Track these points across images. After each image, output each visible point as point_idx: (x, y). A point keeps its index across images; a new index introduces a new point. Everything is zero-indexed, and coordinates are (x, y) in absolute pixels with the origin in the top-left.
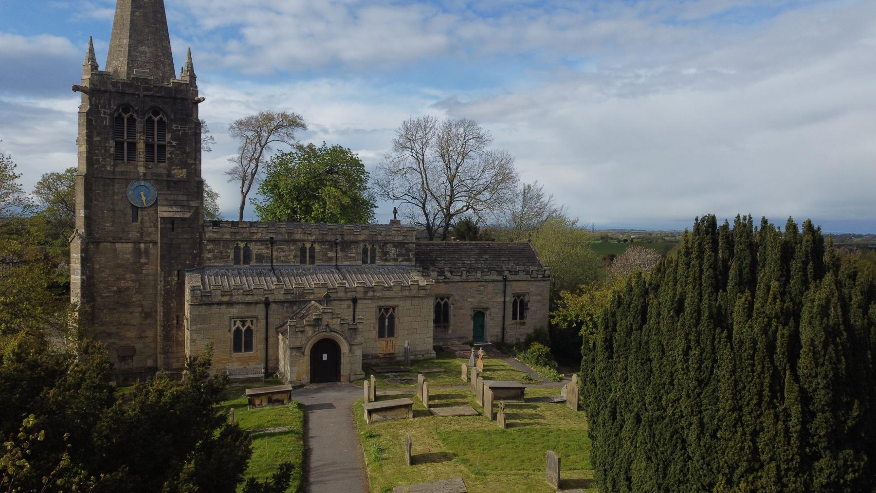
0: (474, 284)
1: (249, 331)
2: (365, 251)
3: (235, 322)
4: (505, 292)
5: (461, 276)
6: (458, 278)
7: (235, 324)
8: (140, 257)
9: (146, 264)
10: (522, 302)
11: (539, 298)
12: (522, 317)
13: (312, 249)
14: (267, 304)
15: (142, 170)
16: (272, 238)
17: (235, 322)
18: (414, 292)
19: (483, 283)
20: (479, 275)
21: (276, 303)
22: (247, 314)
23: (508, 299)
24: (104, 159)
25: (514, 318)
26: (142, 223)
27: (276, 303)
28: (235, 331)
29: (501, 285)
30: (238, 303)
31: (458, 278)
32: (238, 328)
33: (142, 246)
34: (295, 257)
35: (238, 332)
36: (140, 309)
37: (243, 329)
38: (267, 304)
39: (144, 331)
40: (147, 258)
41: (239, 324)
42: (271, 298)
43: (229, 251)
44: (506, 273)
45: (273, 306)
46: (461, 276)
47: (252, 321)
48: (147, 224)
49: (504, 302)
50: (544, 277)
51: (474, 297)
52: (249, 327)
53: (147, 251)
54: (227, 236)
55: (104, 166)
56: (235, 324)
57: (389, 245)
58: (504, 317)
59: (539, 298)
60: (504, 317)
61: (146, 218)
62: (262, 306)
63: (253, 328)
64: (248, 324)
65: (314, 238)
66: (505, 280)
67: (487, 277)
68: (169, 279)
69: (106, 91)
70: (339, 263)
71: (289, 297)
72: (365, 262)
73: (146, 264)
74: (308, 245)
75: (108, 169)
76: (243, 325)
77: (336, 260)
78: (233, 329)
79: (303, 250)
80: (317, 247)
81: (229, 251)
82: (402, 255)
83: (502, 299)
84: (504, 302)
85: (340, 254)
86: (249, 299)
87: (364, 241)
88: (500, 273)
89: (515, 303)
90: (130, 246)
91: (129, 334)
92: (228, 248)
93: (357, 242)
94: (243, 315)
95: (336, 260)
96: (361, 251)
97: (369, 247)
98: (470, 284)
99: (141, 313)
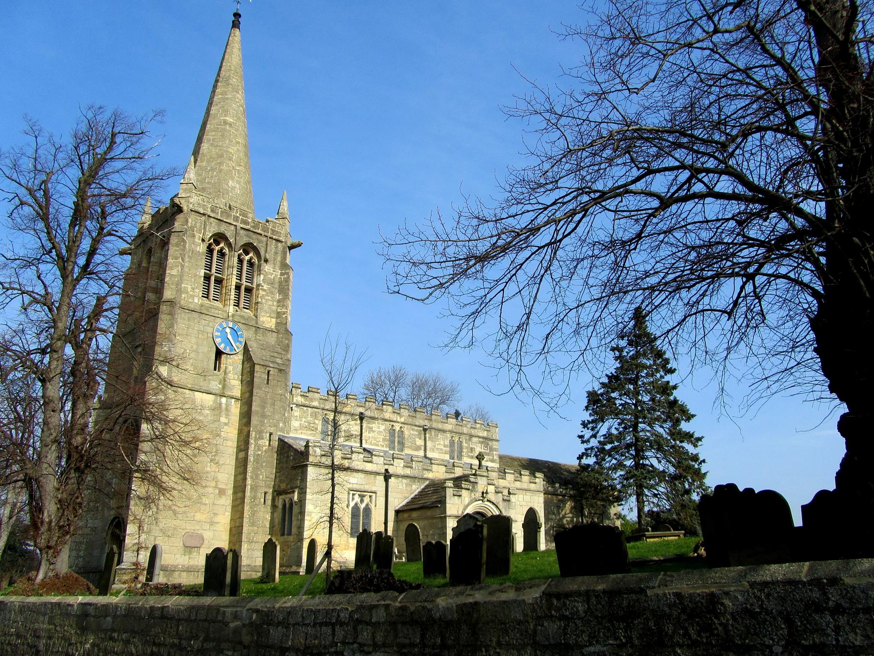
1: (367, 510)
2: (452, 443)
3: (353, 495)
7: (353, 499)
8: (220, 415)
9: (226, 424)
13: (401, 432)
14: (387, 476)
15: (231, 309)
16: (361, 413)
17: (353, 495)
18: (525, 486)
21: (397, 476)
22: (367, 488)
24: (193, 289)
26: (225, 373)
27: (397, 476)
28: (353, 508)
30: (358, 471)
32: (356, 504)
33: (224, 400)
34: (384, 440)
35: (356, 508)
36: (213, 484)
37: (363, 506)
38: (387, 476)
39: (215, 514)
40: (227, 415)
41: (357, 499)
42: (391, 471)
43: (317, 422)
45: (392, 481)
47: (370, 497)
48: (231, 376)
52: (367, 505)
53: (227, 410)
54: (316, 404)
55: (193, 297)
56: (353, 499)
57: (475, 439)
61: (230, 368)
62: (382, 478)
63: (372, 506)
64: (366, 500)
65: (402, 420)
68: (260, 442)
69: (204, 214)
70: (430, 454)
71: (408, 471)
72: (452, 458)
73: (226, 424)
74: (397, 427)
75: (196, 300)
76: (362, 501)
77: (425, 450)
78: (352, 504)
79: (392, 432)
80: (406, 433)
81: (317, 422)
85: (429, 444)
86: (369, 467)
87: (451, 432)
90: (209, 399)
91: (198, 516)
92: (316, 418)
93: (444, 431)
94: (362, 488)
95: (425, 450)
96: (447, 442)
97: (456, 439)
99: (216, 487)
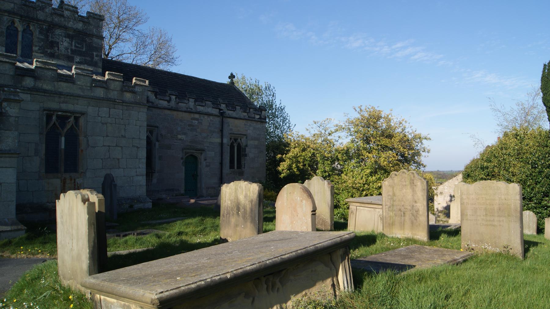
0: (186, 115)
4: (222, 131)
5: (169, 101)
6: (165, 103)
10: (239, 146)
11: (256, 143)
12: (239, 167)
19: (197, 116)
20: (191, 103)
23: (225, 141)
25: (232, 167)
29: (217, 120)
31: (165, 103)
44: (223, 106)
46: (169, 101)
49: (222, 144)
50: (260, 118)
51: (185, 134)
58: (221, 163)
59: (256, 143)
60: (221, 163)
66: (222, 114)
67: (200, 109)
82: (80, 54)
83: (218, 140)
84: (222, 144)
88: (216, 105)
89: (232, 147)
98: (181, 114)
